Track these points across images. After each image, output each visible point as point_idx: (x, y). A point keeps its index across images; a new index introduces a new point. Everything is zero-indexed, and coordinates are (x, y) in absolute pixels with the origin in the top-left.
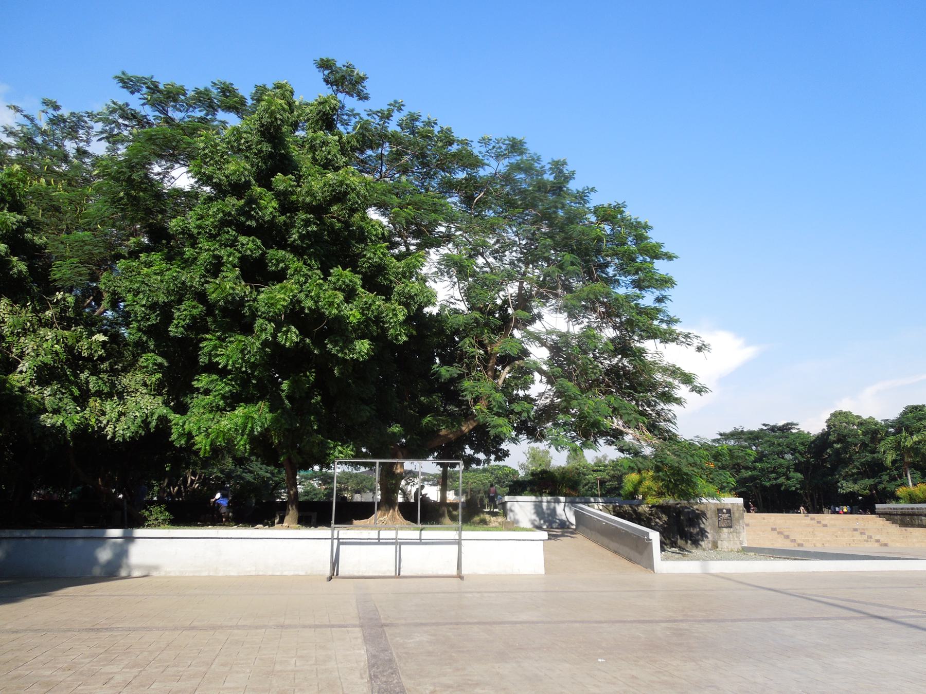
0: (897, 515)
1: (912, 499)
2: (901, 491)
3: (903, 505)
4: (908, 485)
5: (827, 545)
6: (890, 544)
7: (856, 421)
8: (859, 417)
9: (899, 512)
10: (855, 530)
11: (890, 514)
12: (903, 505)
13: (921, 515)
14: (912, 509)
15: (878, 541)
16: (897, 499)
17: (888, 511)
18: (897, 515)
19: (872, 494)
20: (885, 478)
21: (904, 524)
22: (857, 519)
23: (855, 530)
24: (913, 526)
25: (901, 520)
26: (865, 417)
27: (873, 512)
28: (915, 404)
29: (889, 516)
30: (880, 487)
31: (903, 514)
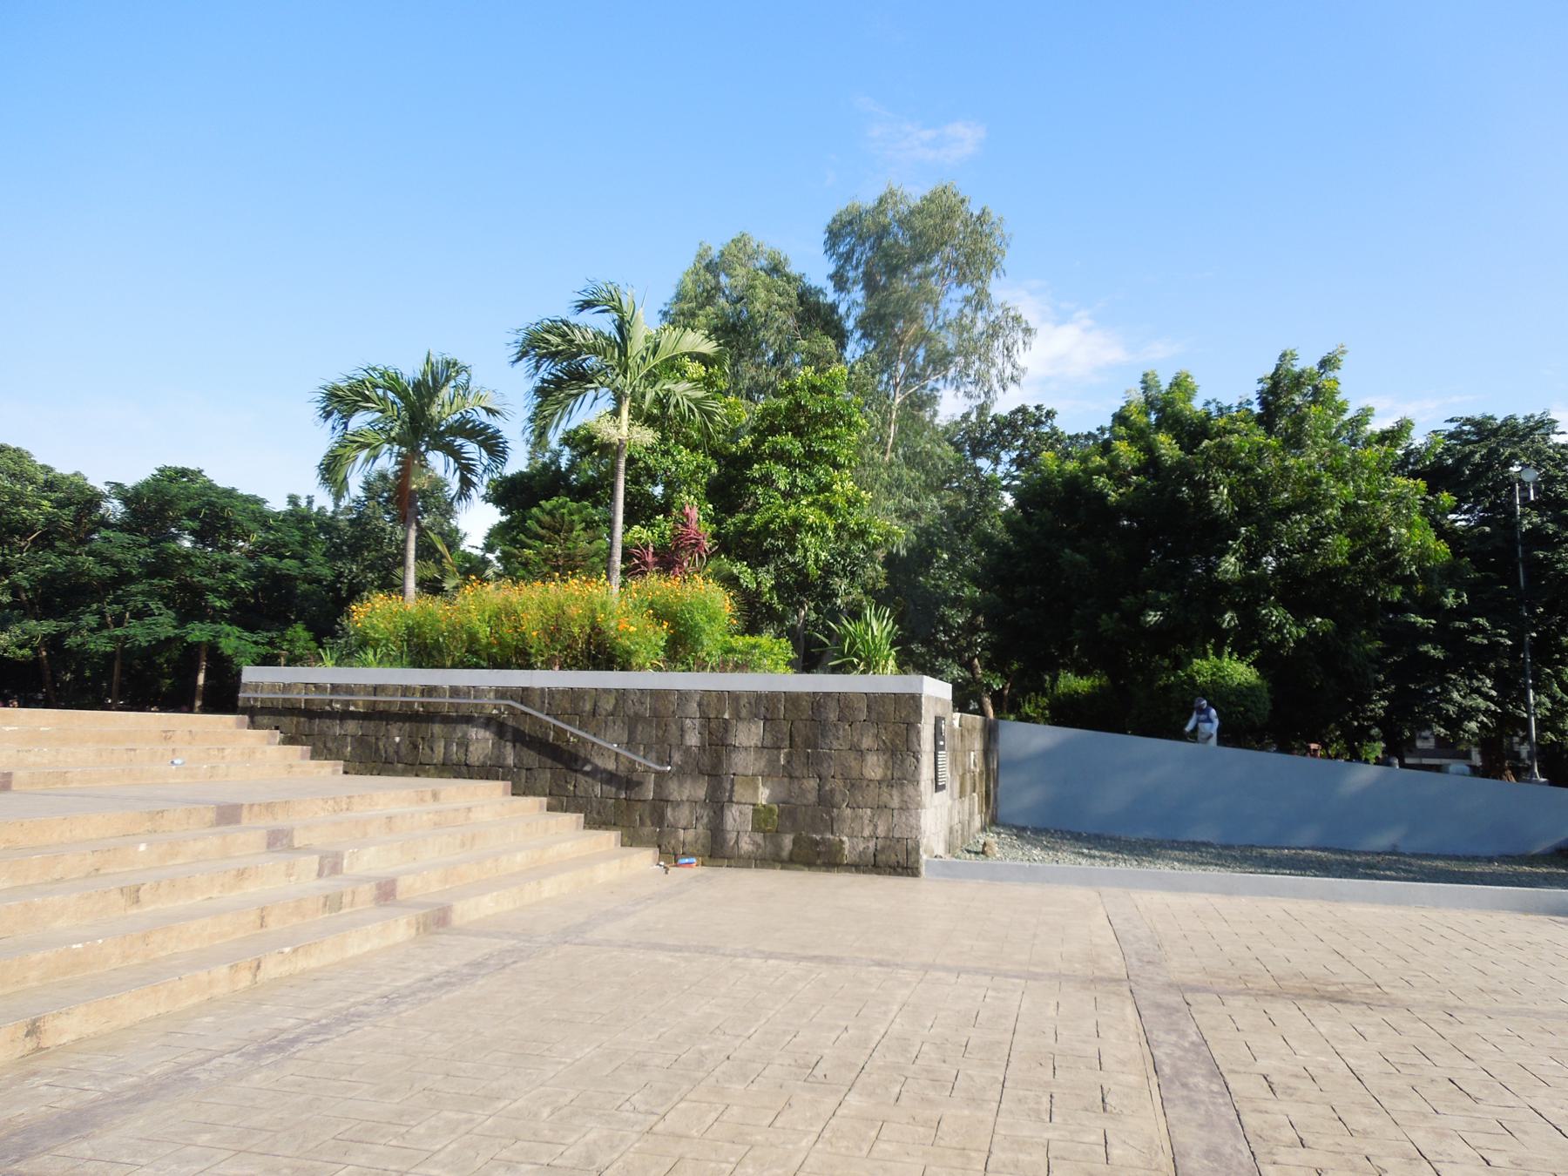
0: (345, 715)
1: (422, 649)
2: (373, 613)
3: (369, 674)
4: (402, 592)
5: (66, 1028)
6: (468, 911)
7: (41, 478)
8: (47, 469)
9: (359, 703)
10: (228, 815)
11: (310, 713)
12: (369, 674)
13: (468, 720)
14: (429, 691)
15: (386, 892)
16: (356, 649)
17: (301, 697)
18: (345, 715)
19: (37, 660)
20: (91, 620)
21: (371, 759)
22: (167, 736)
23: (228, 815)
24: (412, 764)
25: (360, 741)
26: (63, 467)
27: (223, 697)
28: (179, 464)
29: (302, 721)
30: (72, 641)
31: (375, 715)
